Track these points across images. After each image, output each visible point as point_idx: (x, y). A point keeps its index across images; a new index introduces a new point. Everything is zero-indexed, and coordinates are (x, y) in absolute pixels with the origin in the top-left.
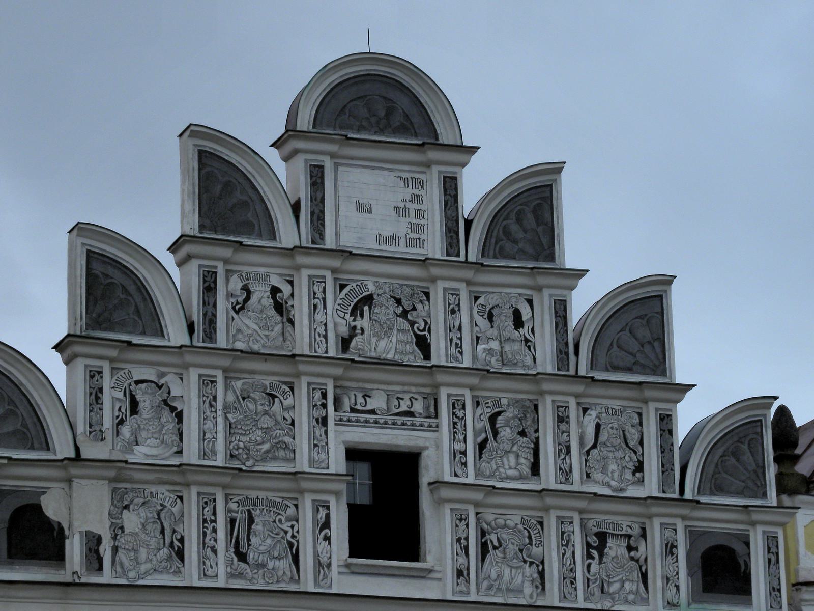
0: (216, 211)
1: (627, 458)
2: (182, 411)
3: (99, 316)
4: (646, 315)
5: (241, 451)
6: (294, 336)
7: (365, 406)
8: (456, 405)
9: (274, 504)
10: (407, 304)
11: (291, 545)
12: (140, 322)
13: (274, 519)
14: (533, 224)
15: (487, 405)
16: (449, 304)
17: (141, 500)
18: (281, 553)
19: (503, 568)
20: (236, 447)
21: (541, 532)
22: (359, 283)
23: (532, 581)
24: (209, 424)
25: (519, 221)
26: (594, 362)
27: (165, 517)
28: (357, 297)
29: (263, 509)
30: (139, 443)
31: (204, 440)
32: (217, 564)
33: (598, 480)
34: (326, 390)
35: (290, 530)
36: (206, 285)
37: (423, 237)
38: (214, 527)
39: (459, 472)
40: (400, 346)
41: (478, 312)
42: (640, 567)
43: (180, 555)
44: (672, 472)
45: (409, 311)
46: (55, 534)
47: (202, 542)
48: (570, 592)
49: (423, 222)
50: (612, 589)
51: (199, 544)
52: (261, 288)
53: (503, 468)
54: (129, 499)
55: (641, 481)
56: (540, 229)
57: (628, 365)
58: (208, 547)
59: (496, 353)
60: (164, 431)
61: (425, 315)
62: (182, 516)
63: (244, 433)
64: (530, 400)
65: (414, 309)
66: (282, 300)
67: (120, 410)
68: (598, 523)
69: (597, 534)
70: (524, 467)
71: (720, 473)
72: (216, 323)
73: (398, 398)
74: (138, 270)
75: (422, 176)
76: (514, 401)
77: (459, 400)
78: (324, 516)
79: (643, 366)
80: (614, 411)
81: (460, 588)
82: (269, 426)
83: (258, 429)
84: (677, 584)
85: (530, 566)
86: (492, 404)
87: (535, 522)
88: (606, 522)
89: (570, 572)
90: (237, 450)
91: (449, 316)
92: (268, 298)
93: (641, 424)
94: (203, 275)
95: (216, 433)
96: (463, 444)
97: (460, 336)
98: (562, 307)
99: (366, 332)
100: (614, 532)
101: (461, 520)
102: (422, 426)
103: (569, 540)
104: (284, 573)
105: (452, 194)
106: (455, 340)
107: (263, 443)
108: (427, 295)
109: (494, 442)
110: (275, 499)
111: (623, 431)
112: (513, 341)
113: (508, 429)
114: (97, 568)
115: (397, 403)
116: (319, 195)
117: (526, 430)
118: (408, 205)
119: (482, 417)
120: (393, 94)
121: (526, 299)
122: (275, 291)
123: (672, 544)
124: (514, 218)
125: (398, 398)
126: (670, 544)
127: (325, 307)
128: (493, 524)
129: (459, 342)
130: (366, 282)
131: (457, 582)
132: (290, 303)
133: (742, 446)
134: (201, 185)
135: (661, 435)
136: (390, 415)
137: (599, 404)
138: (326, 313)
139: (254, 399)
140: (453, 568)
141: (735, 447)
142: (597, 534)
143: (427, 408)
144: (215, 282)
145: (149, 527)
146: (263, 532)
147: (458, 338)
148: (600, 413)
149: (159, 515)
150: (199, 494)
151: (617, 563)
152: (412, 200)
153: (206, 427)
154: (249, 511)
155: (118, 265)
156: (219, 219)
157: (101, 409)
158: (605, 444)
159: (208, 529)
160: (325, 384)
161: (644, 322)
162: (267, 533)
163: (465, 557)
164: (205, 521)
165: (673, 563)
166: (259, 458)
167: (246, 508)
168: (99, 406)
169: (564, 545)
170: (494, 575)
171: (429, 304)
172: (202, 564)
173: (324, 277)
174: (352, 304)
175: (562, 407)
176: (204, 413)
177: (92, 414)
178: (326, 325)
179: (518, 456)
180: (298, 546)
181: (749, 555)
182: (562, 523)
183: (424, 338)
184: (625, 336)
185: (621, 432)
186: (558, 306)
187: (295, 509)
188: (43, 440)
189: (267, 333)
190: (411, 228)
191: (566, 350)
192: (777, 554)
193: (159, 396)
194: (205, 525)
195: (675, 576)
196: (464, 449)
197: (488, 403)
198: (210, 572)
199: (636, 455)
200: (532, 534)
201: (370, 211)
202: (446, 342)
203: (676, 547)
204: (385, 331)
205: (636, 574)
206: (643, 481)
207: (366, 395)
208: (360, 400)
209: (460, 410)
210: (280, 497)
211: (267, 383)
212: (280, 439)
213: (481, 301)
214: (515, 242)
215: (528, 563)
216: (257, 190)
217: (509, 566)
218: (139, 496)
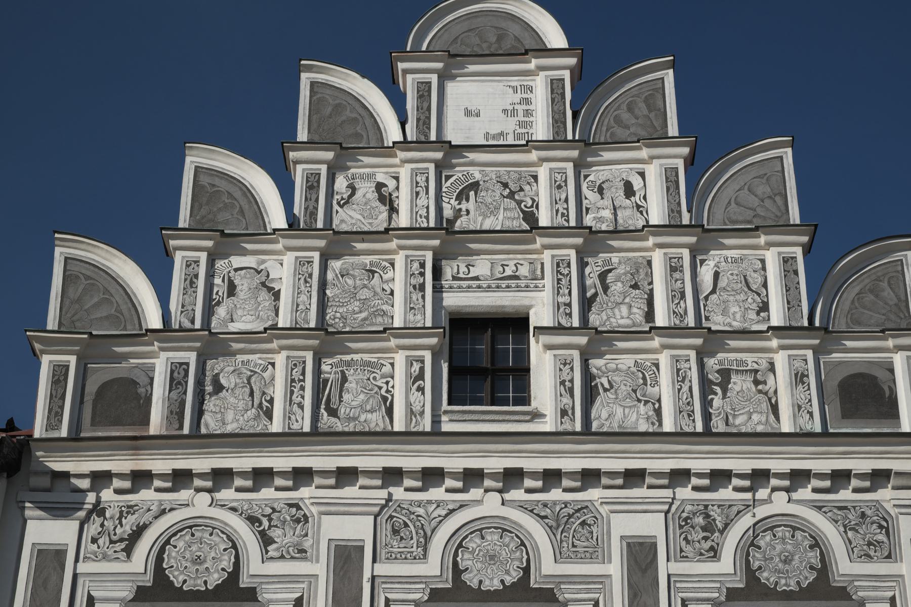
0: (325, 128)
1: (750, 300)
2: (279, 290)
3: (203, 217)
4: (766, 174)
5: (337, 320)
6: (397, 221)
7: (468, 274)
8: (561, 265)
9: (369, 364)
11: (385, 399)
12: (244, 220)
13: (368, 376)
14: (645, 111)
15: (597, 264)
16: (556, 181)
17: (232, 368)
18: (374, 406)
19: (615, 408)
20: (332, 317)
21: (657, 373)
22: (465, 173)
23: (647, 418)
24: (303, 298)
25: (630, 109)
26: (711, 219)
27: (255, 382)
28: (463, 185)
29: (357, 369)
30: (234, 320)
31: (297, 311)
32: (303, 418)
33: (718, 322)
34: (424, 261)
35: (385, 386)
36: (308, 185)
37: (530, 132)
38: (302, 385)
41: (587, 187)
42: (770, 399)
43: (269, 415)
44: (800, 308)
45: (517, 192)
46: (142, 402)
47: (289, 399)
48: (688, 424)
49: (531, 119)
50: (738, 422)
51: (285, 402)
52: (366, 185)
53: (615, 318)
54: (219, 368)
56: (652, 115)
57: (749, 218)
58: (294, 403)
59: (607, 220)
60: (260, 308)
61: (533, 194)
62: (273, 379)
63: (341, 304)
64: (643, 257)
65: (521, 190)
66: (386, 193)
67: (217, 293)
70: (637, 316)
71: (856, 308)
72: (317, 215)
73: (503, 265)
74: (245, 179)
75: (530, 83)
76: (626, 259)
77: (564, 260)
78: (418, 370)
80: (733, 259)
82: (368, 297)
83: (357, 300)
84: (810, 411)
85: (645, 405)
86: (602, 262)
87: (649, 364)
88: (729, 359)
89: (687, 406)
90: (334, 320)
92: (373, 192)
93: (764, 268)
94: (307, 176)
95: (310, 304)
97: (565, 206)
98: (674, 174)
99: (472, 213)
100: (738, 368)
102: (527, 287)
103: (685, 376)
104: (377, 424)
105: (559, 92)
106: (561, 210)
107: (361, 312)
108: (535, 178)
109: (604, 295)
110: (370, 359)
111: (745, 277)
112: (625, 208)
113: (619, 284)
114: (177, 428)
115: (501, 269)
116: (425, 105)
117: (639, 283)
119: (591, 275)
120: (503, 24)
121: (637, 172)
122: (380, 186)
123: (802, 373)
124: (625, 108)
125: (503, 265)
126: (800, 374)
127: (427, 193)
128: (603, 368)
129: (565, 211)
130: (471, 172)
131: (561, 421)
132: (395, 195)
133: (881, 283)
134: (312, 108)
135: (785, 276)
136: (494, 280)
137: (718, 255)
138: (428, 198)
139: (352, 275)
140: (556, 408)
141: (873, 285)
142: (718, 372)
143: (533, 272)
144: (318, 182)
145: (237, 392)
146: (356, 389)
147: (564, 209)
148: (718, 262)
150: (288, 357)
151: (744, 397)
152: (520, 103)
153: (301, 299)
154: (342, 372)
155: (226, 177)
156: (328, 134)
158: (724, 289)
159: (295, 387)
160: (424, 256)
161: (764, 181)
162: (359, 389)
163: (569, 397)
164: (293, 381)
165: (805, 391)
166: (356, 325)
167: (339, 369)
168: (193, 289)
169: (680, 381)
170: (604, 415)
171: (537, 185)
172: (287, 418)
173: (428, 169)
174: (458, 191)
175: (675, 258)
176: (299, 288)
177: (185, 296)
178: (428, 208)
179: (630, 307)
180: (392, 400)
182: (677, 361)
183: (532, 213)
185: (742, 277)
186: (669, 174)
187: (390, 366)
188: (136, 322)
189: (371, 221)
190: (519, 125)
191: (679, 209)
193: (258, 279)
194: (293, 384)
195: (807, 403)
196: (569, 301)
197: (598, 262)
199: (759, 297)
200: (647, 375)
201: (478, 115)
202: (552, 213)
203: (807, 376)
204: (494, 211)
205: (765, 406)
206: (769, 319)
207: (469, 265)
208: (463, 269)
209: (564, 268)
210: (375, 358)
212: (379, 308)
213: (591, 178)
214: (627, 127)
215: (643, 402)
216: (366, 108)
217: (622, 406)
218: (230, 365)
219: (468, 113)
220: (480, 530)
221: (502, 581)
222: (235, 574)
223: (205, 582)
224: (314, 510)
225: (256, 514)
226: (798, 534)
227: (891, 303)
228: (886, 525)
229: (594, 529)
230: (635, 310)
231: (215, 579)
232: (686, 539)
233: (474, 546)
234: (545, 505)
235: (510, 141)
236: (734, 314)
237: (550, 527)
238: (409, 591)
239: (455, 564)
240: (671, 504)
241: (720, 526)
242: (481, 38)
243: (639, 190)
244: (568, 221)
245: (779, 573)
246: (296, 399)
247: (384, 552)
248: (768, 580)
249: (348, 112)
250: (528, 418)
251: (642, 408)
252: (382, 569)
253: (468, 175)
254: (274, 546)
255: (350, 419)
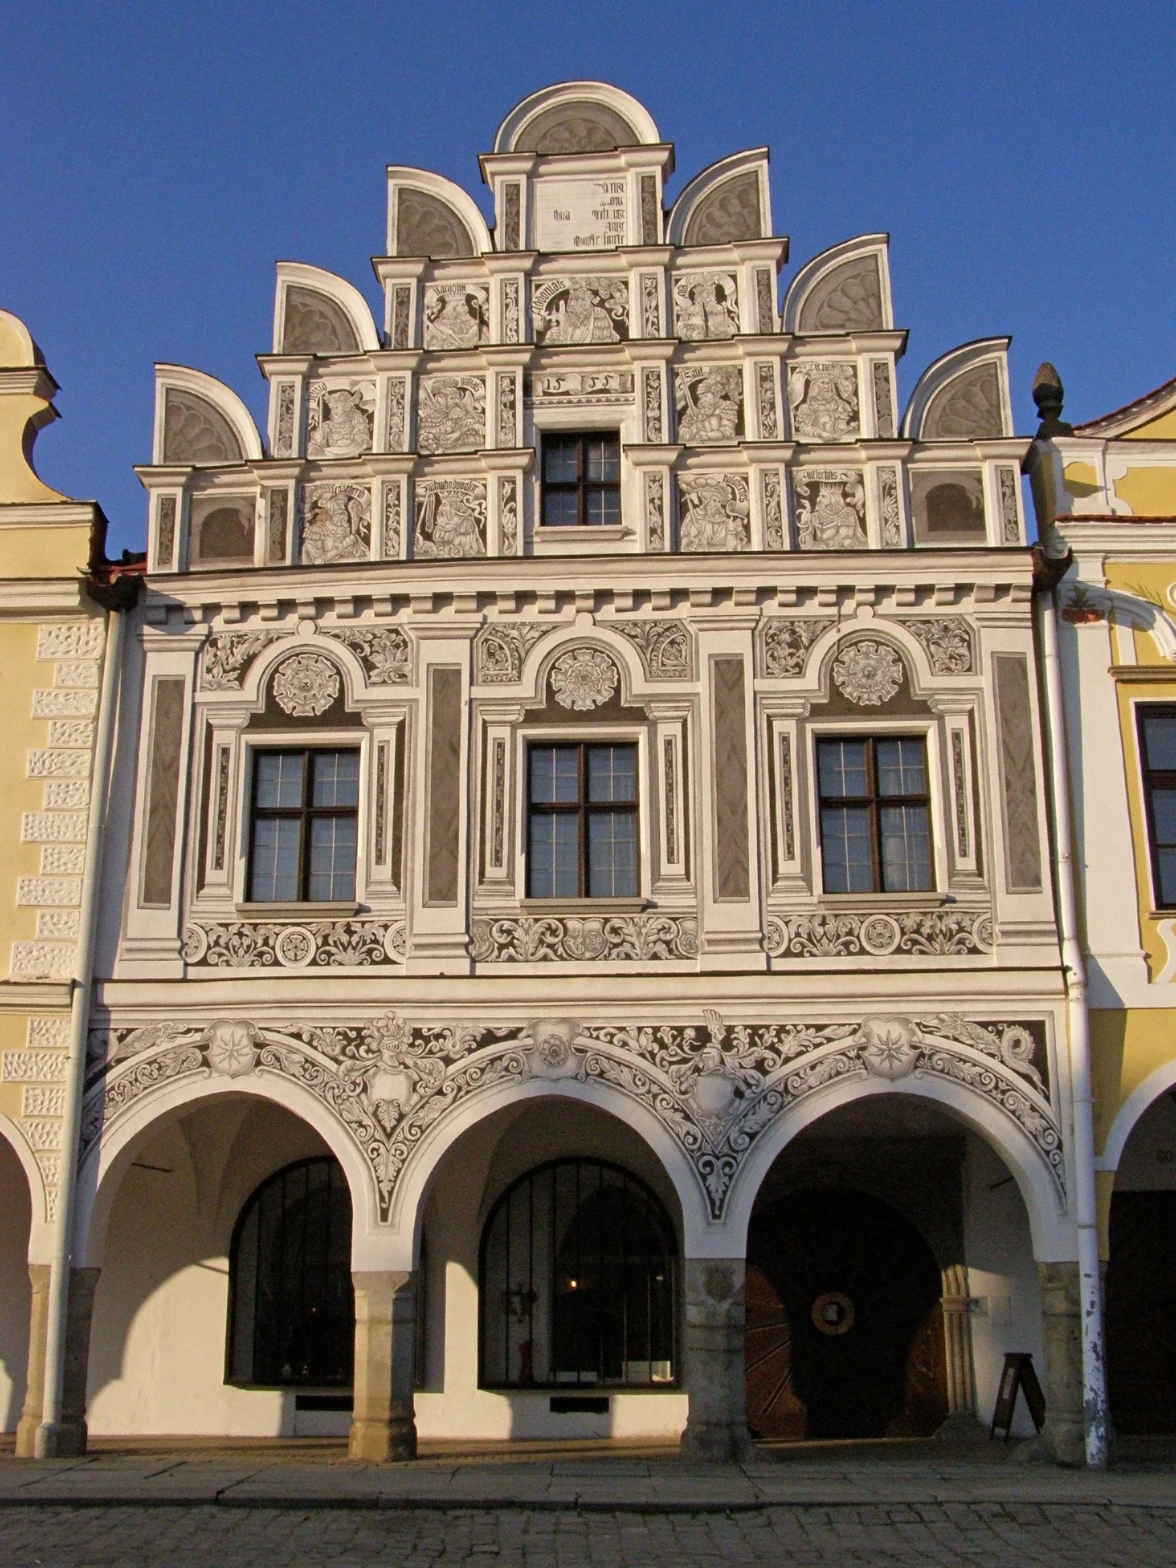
1: (840, 409)
2: (373, 413)
3: (296, 340)
10: (603, 294)
11: (478, 521)
14: (738, 209)
24: (396, 420)
25: (723, 206)
39: (653, 437)
40: (598, 333)
42: (858, 512)
43: (367, 540)
49: (622, 220)
55: (858, 429)
56: (745, 212)
57: (840, 322)
62: (370, 504)
65: (612, 297)
68: (809, 474)
69: (808, 485)
79: (856, 321)
81: (653, 545)
87: (738, 478)
91: (645, 298)
93: (855, 375)
96: (657, 411)
101: (654, 481)
107: (453, 432)
108: (626, 284)
111: (836, 385)
113: (709, 395)
118: (606, 208)
122: (470, 298)
127: (517, 305)
132: (484, 307)
139: (446, 396)
142: (808, 485)
143: (623, 384)
149: (346, 506)
150: (383, 482)
154: (437, 495)
157: (291, 418)
164: (388, 506)
170: (694, 532)
173: (517, 279)
178: (517, 320)
179: (720, 419)
181: (982, 491)
184: (837, 297)
188: (237, 451)
192: (1013, 487)
198: (391, 552)
201: (568, 218)
203: (895, 488)
204: (583, 321)
205: (853, 519)
208: (554, 383)
211: (459, 379)
213: (681, 283)
214: (719, 226)
219: (558, 216)
220: (573, 651)
221: (594, 701)
222: (340, 701)
223: (313, 708)
224: (413, 634)
225: (357, 641)
226: (882, 649)
227: (983, 409)
228: (966, 637)
229: (683, 647)
230: (725, 422)
231: (323, 705)
232: (772, 656)
233: (567, 667)
234: (635, 624)
235: (601, 246)
236: (824, 424)
237: (640, 647)
238: (505, 713)
239: (549, 685)
240: (758, 622)
241: (806, 642)
242: (571, 132)
243: (731, 294)
244: (658, 330)
245: (863, 687)
246: (392, 524)
247: (481, 674)
248: (851, 694)
249: (436, 221)
250: (618, 536)
251: (731, 525)
252: (479, 692)
253: (557, 283)
254: (376, 671)
255: (445, 543)
